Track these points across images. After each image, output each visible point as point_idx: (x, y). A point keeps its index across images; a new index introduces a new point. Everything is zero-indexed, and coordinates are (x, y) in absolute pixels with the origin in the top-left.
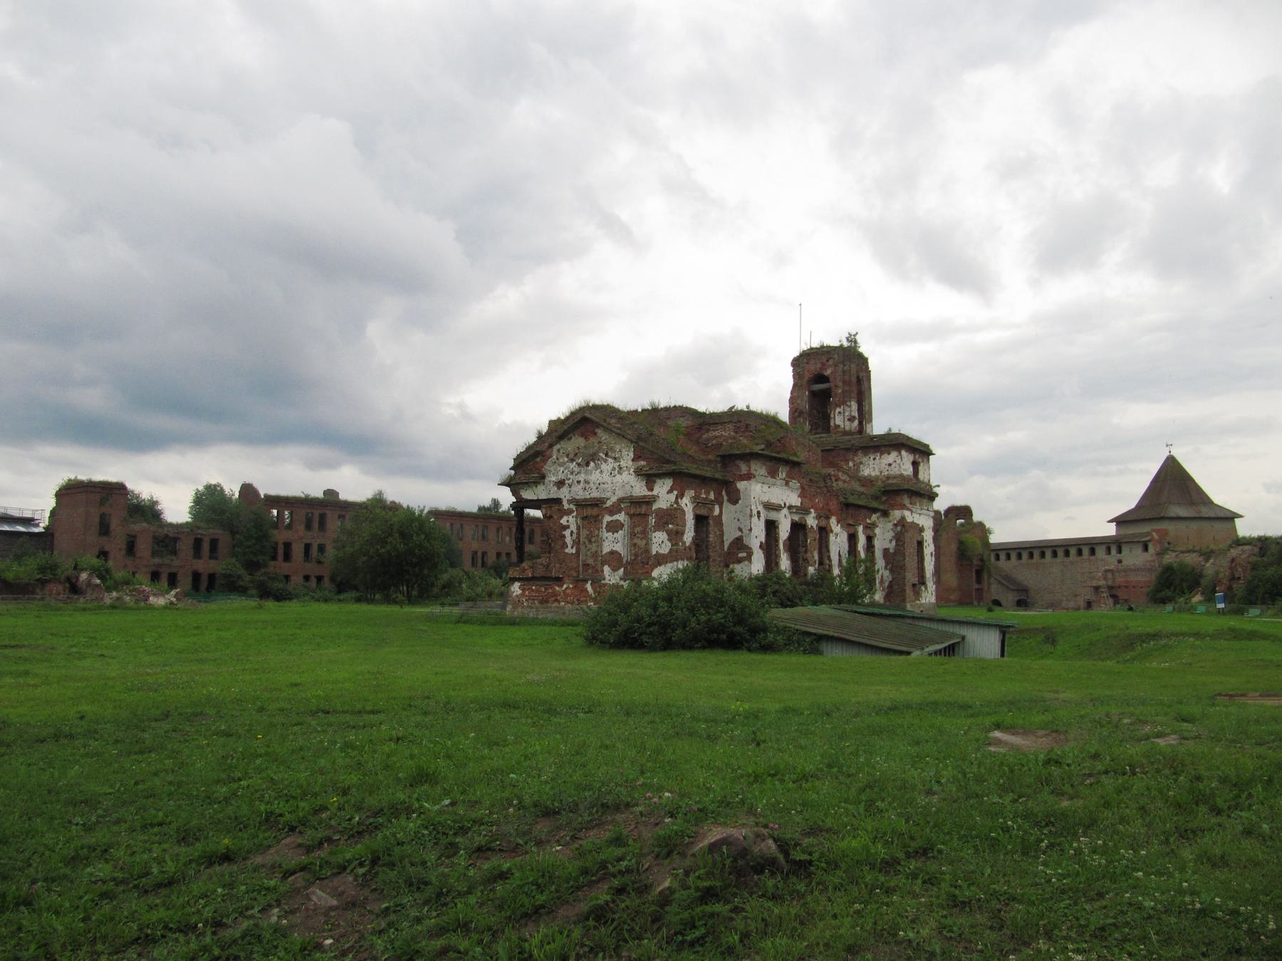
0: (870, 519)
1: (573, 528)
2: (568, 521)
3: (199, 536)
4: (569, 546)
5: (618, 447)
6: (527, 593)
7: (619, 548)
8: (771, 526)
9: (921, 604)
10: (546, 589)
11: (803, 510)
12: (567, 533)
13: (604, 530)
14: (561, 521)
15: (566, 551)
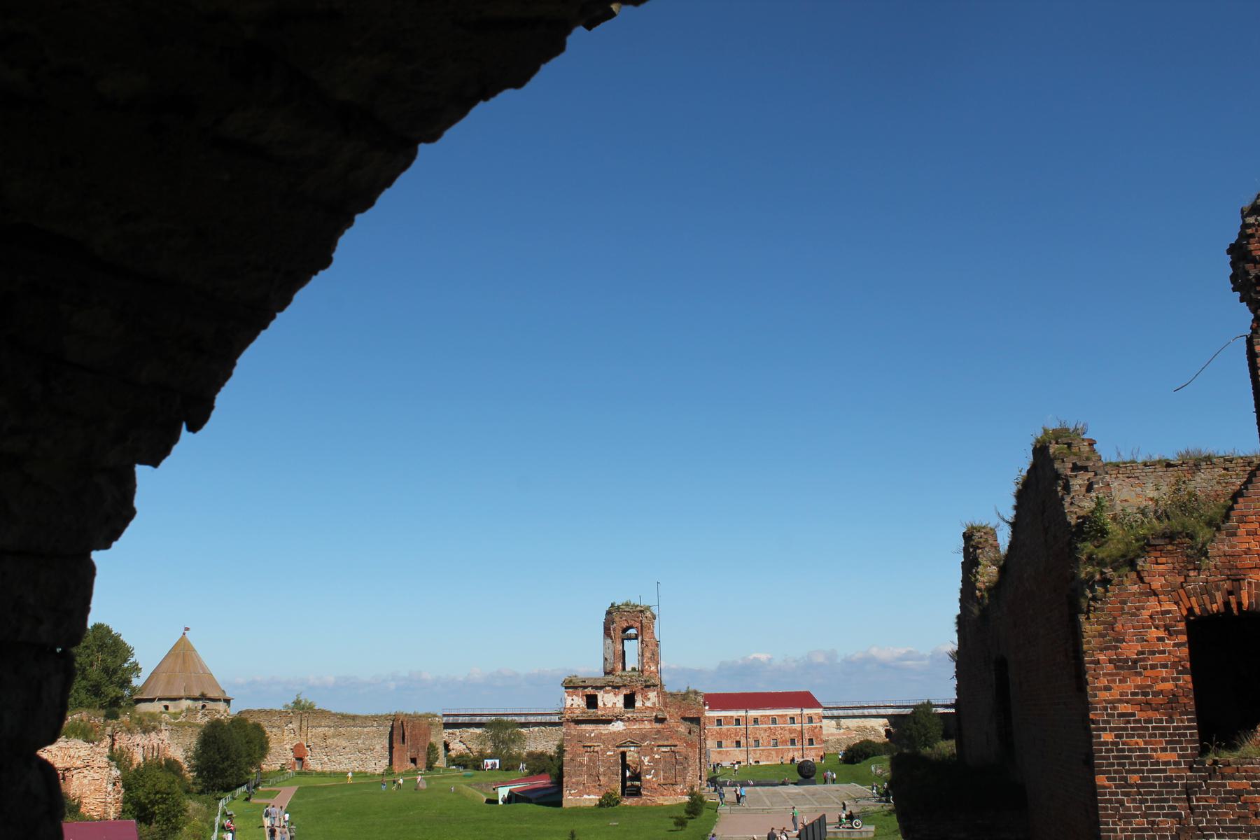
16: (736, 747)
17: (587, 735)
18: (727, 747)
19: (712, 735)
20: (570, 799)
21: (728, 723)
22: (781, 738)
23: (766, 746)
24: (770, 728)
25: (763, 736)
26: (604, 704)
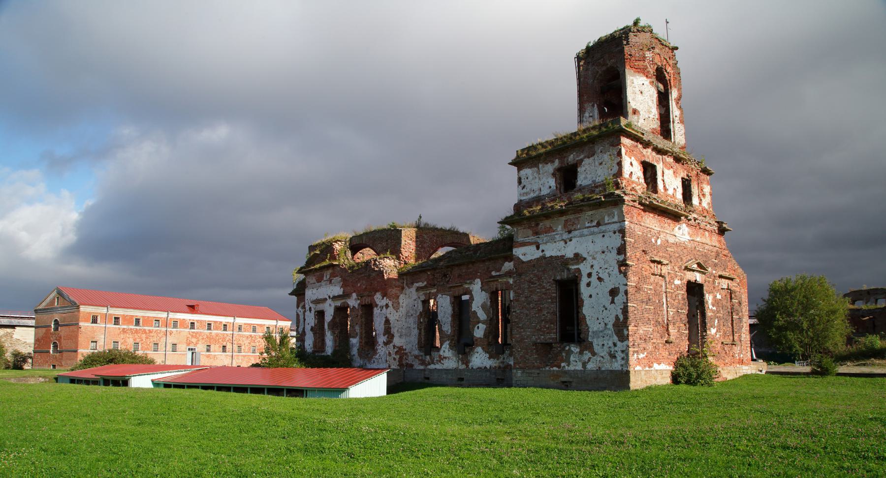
0: (499, 270)
8: (320, 314)
9: (566, 372)
11: (346, 295)
16: (223, 352)
17: (653, 240)
18: (215, 351)
19: (203, 339)
20: (640, 371)
21: (217, 329)
22: (259, 345)
23: (247, 352)
24: (251, 336)
25: (245, 343)
26: (664, 186)
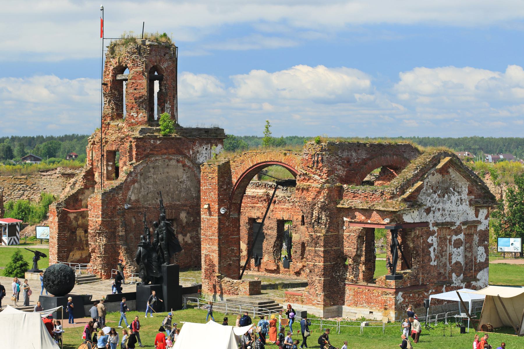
1: (435, 245)
2: (432, 240)
3: (256, 279)
4: (433, 259)
5: (460, 184)
6: (407, 300)
7: (461, 259)
10: (419, 295)
12: (431, 250)
13: (453, 246)
14: (428, 241)
15: (431, 263)
